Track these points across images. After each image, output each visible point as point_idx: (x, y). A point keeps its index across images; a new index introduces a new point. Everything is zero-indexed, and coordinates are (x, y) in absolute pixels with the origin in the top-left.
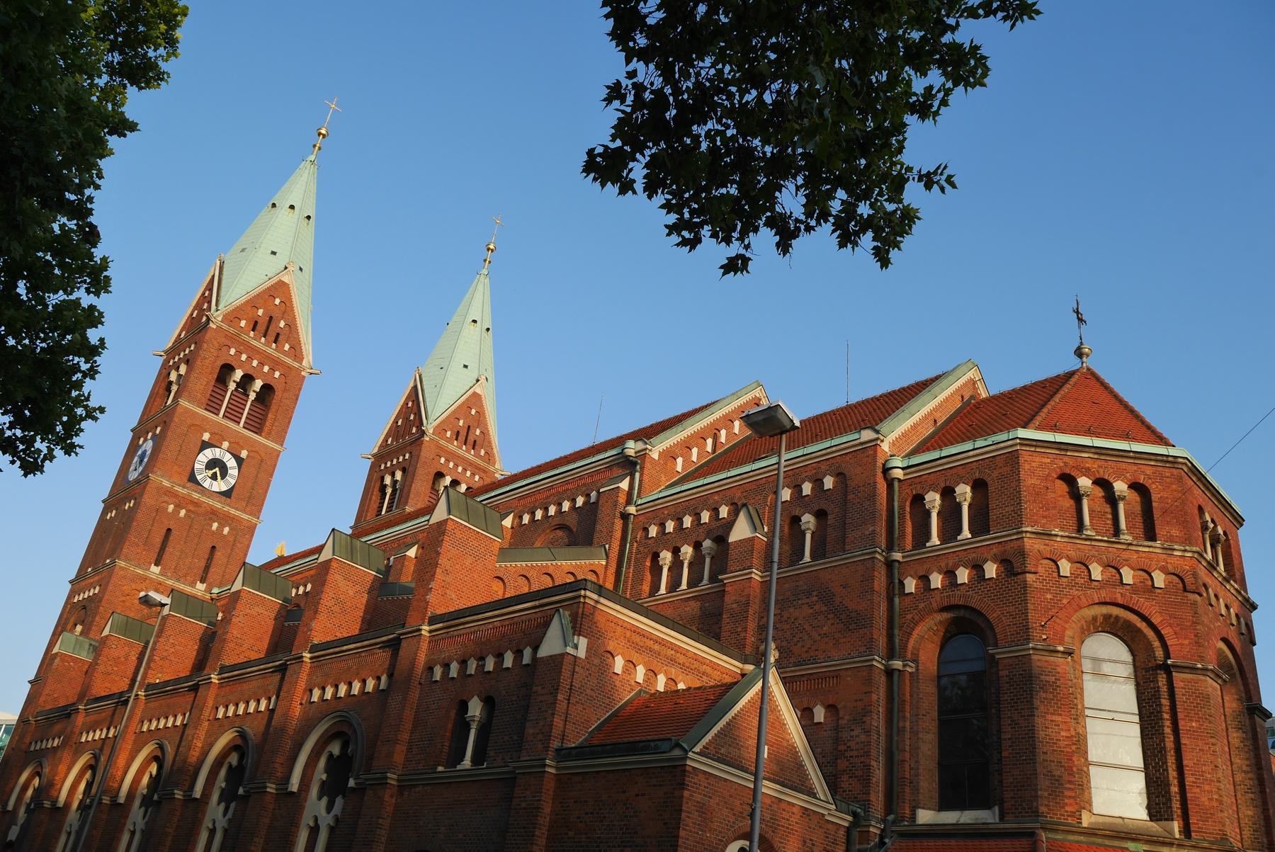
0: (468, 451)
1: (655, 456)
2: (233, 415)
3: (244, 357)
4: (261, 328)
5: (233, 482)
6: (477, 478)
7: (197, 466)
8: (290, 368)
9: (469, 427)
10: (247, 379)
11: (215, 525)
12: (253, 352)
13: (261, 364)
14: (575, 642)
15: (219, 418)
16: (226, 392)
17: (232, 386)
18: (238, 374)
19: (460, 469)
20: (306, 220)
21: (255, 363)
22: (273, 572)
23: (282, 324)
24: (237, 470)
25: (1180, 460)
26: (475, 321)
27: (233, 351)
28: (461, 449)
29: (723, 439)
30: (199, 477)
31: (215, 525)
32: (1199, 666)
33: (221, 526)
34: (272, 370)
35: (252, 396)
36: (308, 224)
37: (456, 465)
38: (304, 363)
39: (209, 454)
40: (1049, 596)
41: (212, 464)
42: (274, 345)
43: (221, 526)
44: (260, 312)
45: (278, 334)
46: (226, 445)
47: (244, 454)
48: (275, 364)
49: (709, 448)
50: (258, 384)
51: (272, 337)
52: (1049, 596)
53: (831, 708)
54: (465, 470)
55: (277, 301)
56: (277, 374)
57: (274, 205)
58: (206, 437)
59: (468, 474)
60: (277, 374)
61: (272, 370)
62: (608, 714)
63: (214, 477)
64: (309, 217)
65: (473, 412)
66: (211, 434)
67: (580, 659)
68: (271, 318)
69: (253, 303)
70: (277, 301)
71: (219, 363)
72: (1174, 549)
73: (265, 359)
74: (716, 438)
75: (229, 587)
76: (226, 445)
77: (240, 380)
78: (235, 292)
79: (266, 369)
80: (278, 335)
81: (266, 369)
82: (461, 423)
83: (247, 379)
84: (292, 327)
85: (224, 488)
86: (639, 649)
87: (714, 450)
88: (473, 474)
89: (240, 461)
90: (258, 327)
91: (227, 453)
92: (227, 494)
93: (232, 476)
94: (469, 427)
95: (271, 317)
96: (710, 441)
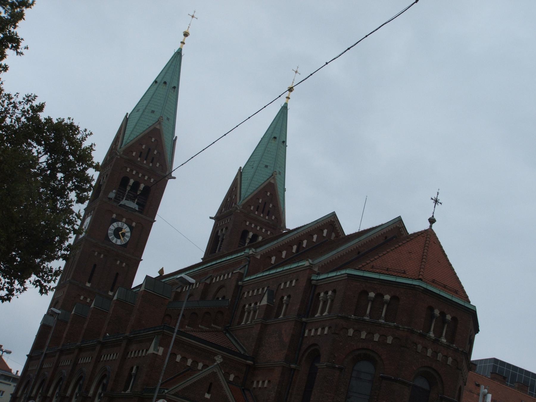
0: (264, 217)
1: (259, 257)
6: (269, 233)
7: (109, 232)
9: (265, 203)
10: (136, 185)
14: (158, 349)
16: (126, 191)
17: (128, 188)
18: (132, 181)
19: (258, 228)
20: (173, 89)
22: (163, 281)
23: (155, 152)
25: (416, 286)
26: (275, 138)
27: (128, 170)
28: (260, 216)
29: (304, 245)
30: (110, 238)
32: (393, 378)
33: (121, 263)
36: (174, 91)
37: (256, 226)
40: (341, 344)
41: (118, 230)
43: (121, 263)
44: (144, 147)
45: (153, 158)
46: (124, 220)
47: (134, 224)
49: (294, 251)
50: (142, 186)
52: (341, 344)
53: (269, 381)
54: (261, 229)
55: (153, 140)
59: (264, 230)
62: (171, 377)
63: (123, 235)
65: (268, 194)
66: (117, 215)
67: (159, 355)
70: (153, 140)
72: (399, 327)
74: (300, 244)
75: (139, 289)
76: (124, 220)
77: (132, 185)
82: (260, 201)
83: (136, 185)
87: (297, 250)
88: (266, 231)
89: (131, 228)
91: (125, 224)
93: (127, 236)
94: (265, 203)
95: (150, 149)
96: (295, 247)
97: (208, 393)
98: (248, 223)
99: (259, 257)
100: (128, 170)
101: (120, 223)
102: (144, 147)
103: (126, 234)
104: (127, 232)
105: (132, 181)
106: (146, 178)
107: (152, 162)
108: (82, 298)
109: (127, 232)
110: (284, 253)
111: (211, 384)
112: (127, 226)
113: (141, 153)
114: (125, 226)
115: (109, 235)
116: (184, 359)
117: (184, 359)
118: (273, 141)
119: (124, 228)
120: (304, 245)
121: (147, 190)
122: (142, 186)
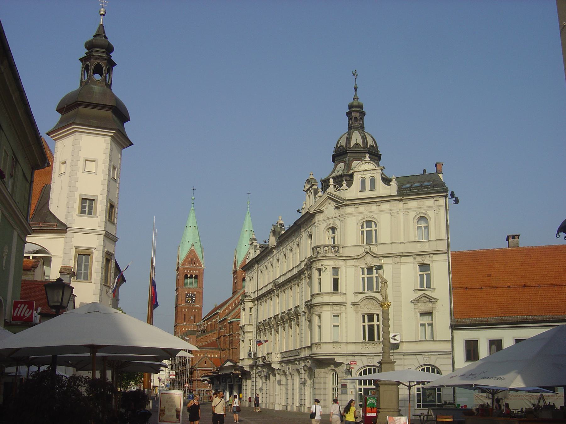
1: (222, 312)
8: (199, 269)
11: (194, 310)
12: (190, 269)
13: (193, 271)
18: (189, 275)
21: (191, 271)
26: (247, 230)
27: (186, 271)
29: (237, 302)
31: (194, 310)
34: (196, 271)
38: (202, 266)
42: (195, 265)
45: (195, 262)
48: (196, 270)
49: (234, 305)
50: (194, 276)
51: (193, 263)
55: (192, 254)
56: (197, 272)
57: (187, 227)
60: (197, 272)
61: (196, 271)
64: (195, 227)
66: (187, 291)
68: (192, 259)
69: (187, 258)
70: (192, 254)
71: (184, 275)
73: (193, 269)
78: (183, 257)
80: (195, 262)
81: (194, 272)
84: (197, 259)
86: (201, 353)
87: (235, 305)
90: (190, 263)
96: (234, 304)
97: (206, 364)
98: (244, 274)
99: (222, 312)
100: (186, 271)
105: (189, 275)
106: (194, 272)
107: (195, 264)
110: (230, 307)
111: (206, 362)
113: (189, 262)
116: (200, 355)
117: (200, 355)
118: (246, 232)
120: (237, 302)
121: (196, 277)
122: (194, 276)
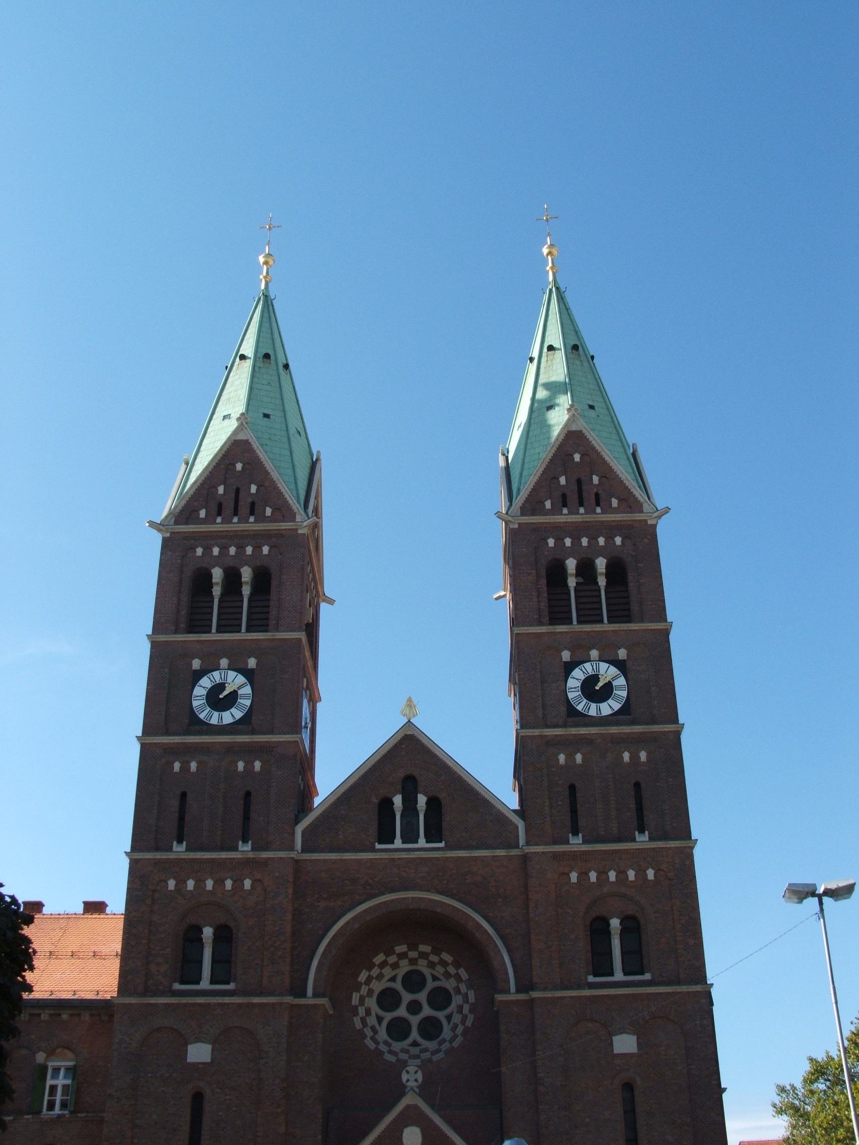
2: (590, 615)
3: (568, 542)
4: (573, 498)
5: (624, 694)
7: (571, 695)
15: (576, 627)
18: (571, 564)
23: (596, 480)
24: (623, 678)
30: (580, 708)
35: (602, 581)
39: (578, 675)
44: (563, 480)
47: (622, 654)
48: (611, 530)
50: (601, 564)
58: (566, 656)
60: (618, 540)
76: (594, 653)
79: (601, 541)
85: (617, 706)
89: (621, 665)
91: (602, 664)
92: (626, 709)
93: (620, 688)
101: (588, 666)
102: (563, 480)
103: (615, 683)
104: (615, 678)
105: (571, 564)
108: (574, 877)
109: (615, 678)
112: (608, 665)
114: (603, 666)
115: (572, 703)
119: (602, 671)
122: (601, 564)
